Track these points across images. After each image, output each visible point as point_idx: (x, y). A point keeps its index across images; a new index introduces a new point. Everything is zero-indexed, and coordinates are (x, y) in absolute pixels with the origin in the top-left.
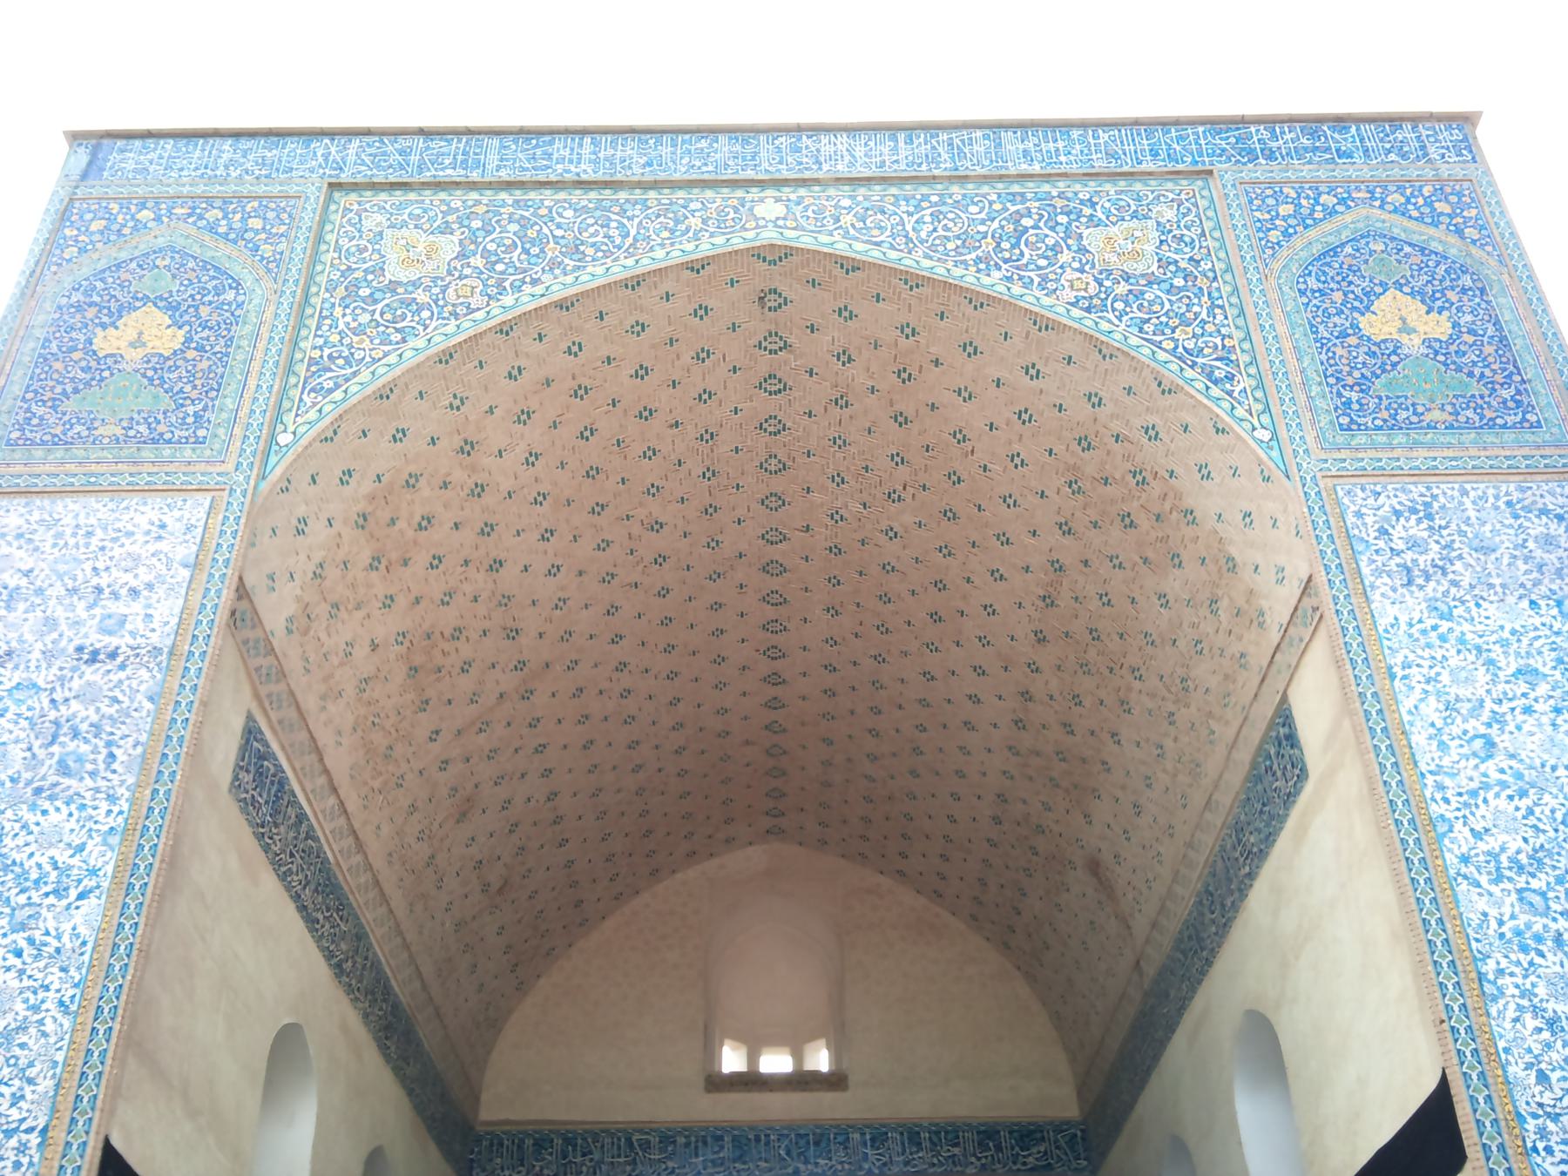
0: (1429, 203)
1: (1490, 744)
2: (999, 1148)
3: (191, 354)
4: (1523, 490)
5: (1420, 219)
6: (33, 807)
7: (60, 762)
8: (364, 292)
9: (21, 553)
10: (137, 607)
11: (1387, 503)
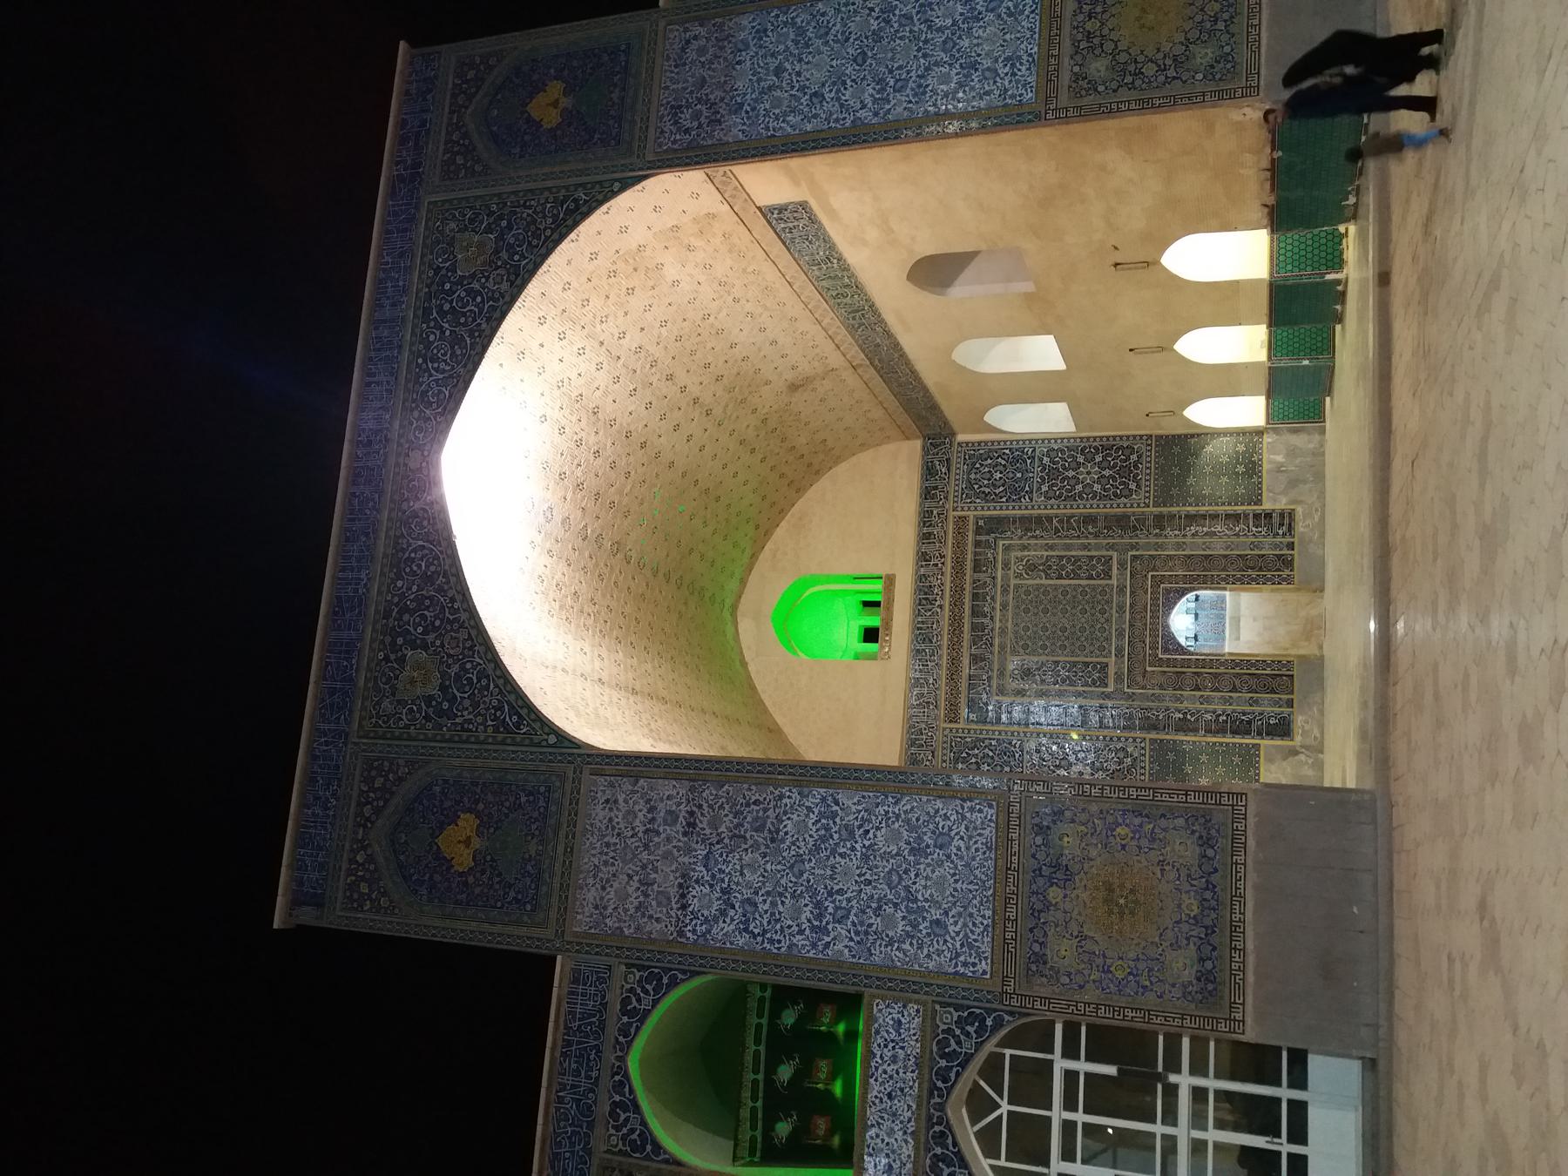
0: (467, 82)
1: (815, 94)
2: (936, 488)
3: (481, 806)
4: (668, 58)
5: (478, 88)
6: (783, 841)
7: (756, 831)
8: (446, 705)
9: (616, 885)
10: (661, 806)
11: (668, 127)
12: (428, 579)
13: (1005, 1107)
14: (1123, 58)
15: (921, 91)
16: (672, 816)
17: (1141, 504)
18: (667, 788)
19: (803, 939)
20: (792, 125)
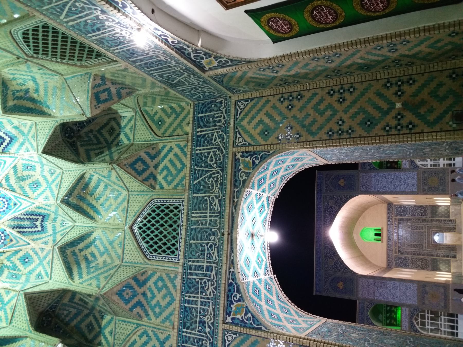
12: (330, 249)
13: (419, 320)
15: (400, 188)
16: (372, 284)
17: (428, 217)
18: (371, 280)
19: (390, 299)
20: (381, 190)
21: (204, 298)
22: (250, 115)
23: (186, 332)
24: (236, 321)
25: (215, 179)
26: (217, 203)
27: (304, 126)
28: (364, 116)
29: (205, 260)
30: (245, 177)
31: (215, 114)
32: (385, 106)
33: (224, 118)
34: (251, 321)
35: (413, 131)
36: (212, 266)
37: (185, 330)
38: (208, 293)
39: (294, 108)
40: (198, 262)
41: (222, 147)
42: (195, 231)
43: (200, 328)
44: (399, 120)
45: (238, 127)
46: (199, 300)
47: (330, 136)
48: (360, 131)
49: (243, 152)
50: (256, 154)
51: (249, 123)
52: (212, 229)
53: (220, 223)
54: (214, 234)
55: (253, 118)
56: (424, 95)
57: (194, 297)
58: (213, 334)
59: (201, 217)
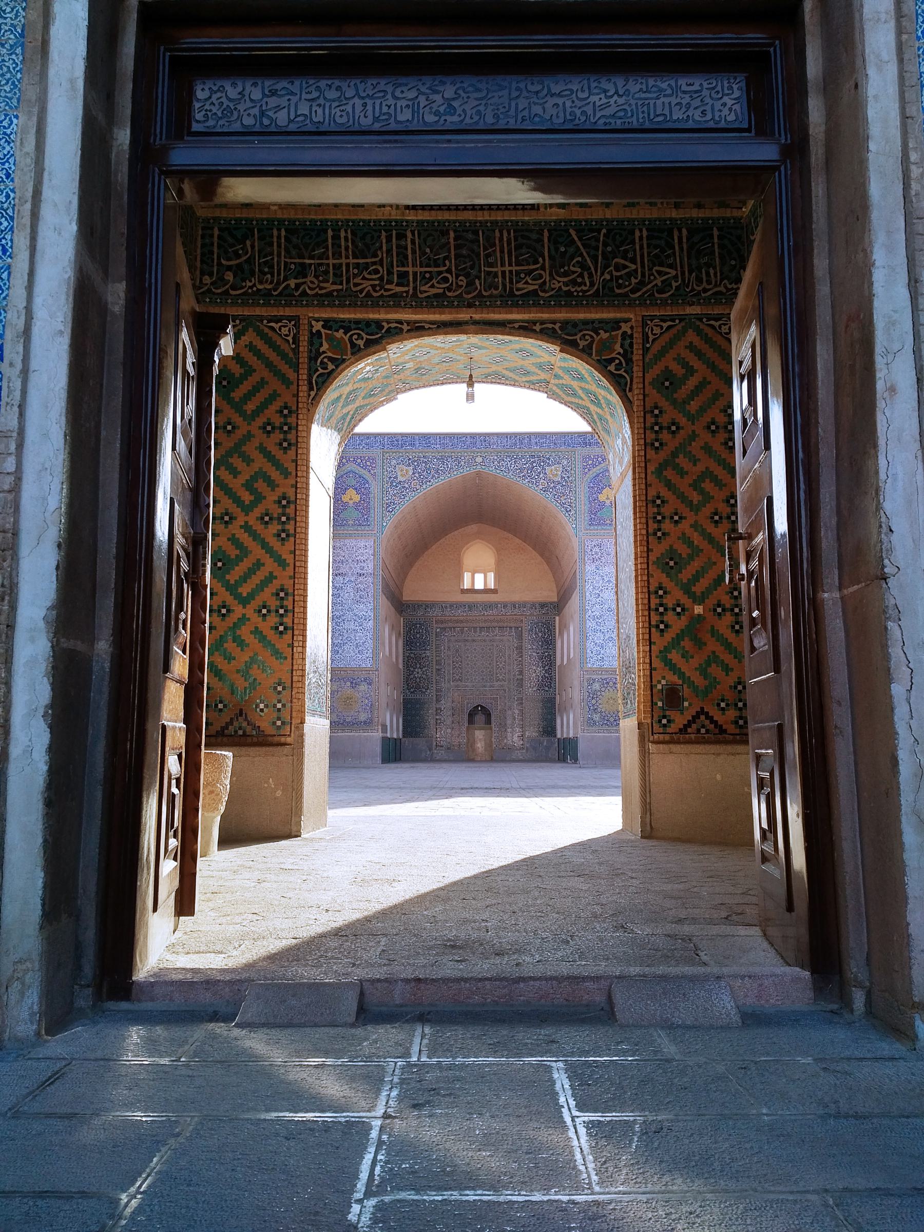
14: (599, 693)
15: (595, 631)
21: (348, 271)
22: (705, 348)
23: (279, 237)
24: (315, 340)
25: (579, 280)
26: (531, 288)
27: (674, 455)
28: (684, 556)
29: (419, 269)
30: (582, 343)
31: (715, 268)
32: (698, 588)
33: (705, 290)
34: (321, 371)
35: (653, 630)
36: (408, 285)
37: (283, 233)
38: (357, 280)
39: (710, 435)
40: (414, 252)
41: (645, 289)
42: (472, 242)
43: (293, 267)
44: (674, 610)
45: (683, 324)
46: (344, 261)
47: (654, 502)
48: (659, 549)
49: (631, 336)
50: (627, 364)
51: (691, 347)
52: (479, 278)
53: (491, 296)
54: (470, 284)
55: (699, 354)
56: (712, 645)
57: (347, 249)
58: (286, 296)
59: (502, 252)
